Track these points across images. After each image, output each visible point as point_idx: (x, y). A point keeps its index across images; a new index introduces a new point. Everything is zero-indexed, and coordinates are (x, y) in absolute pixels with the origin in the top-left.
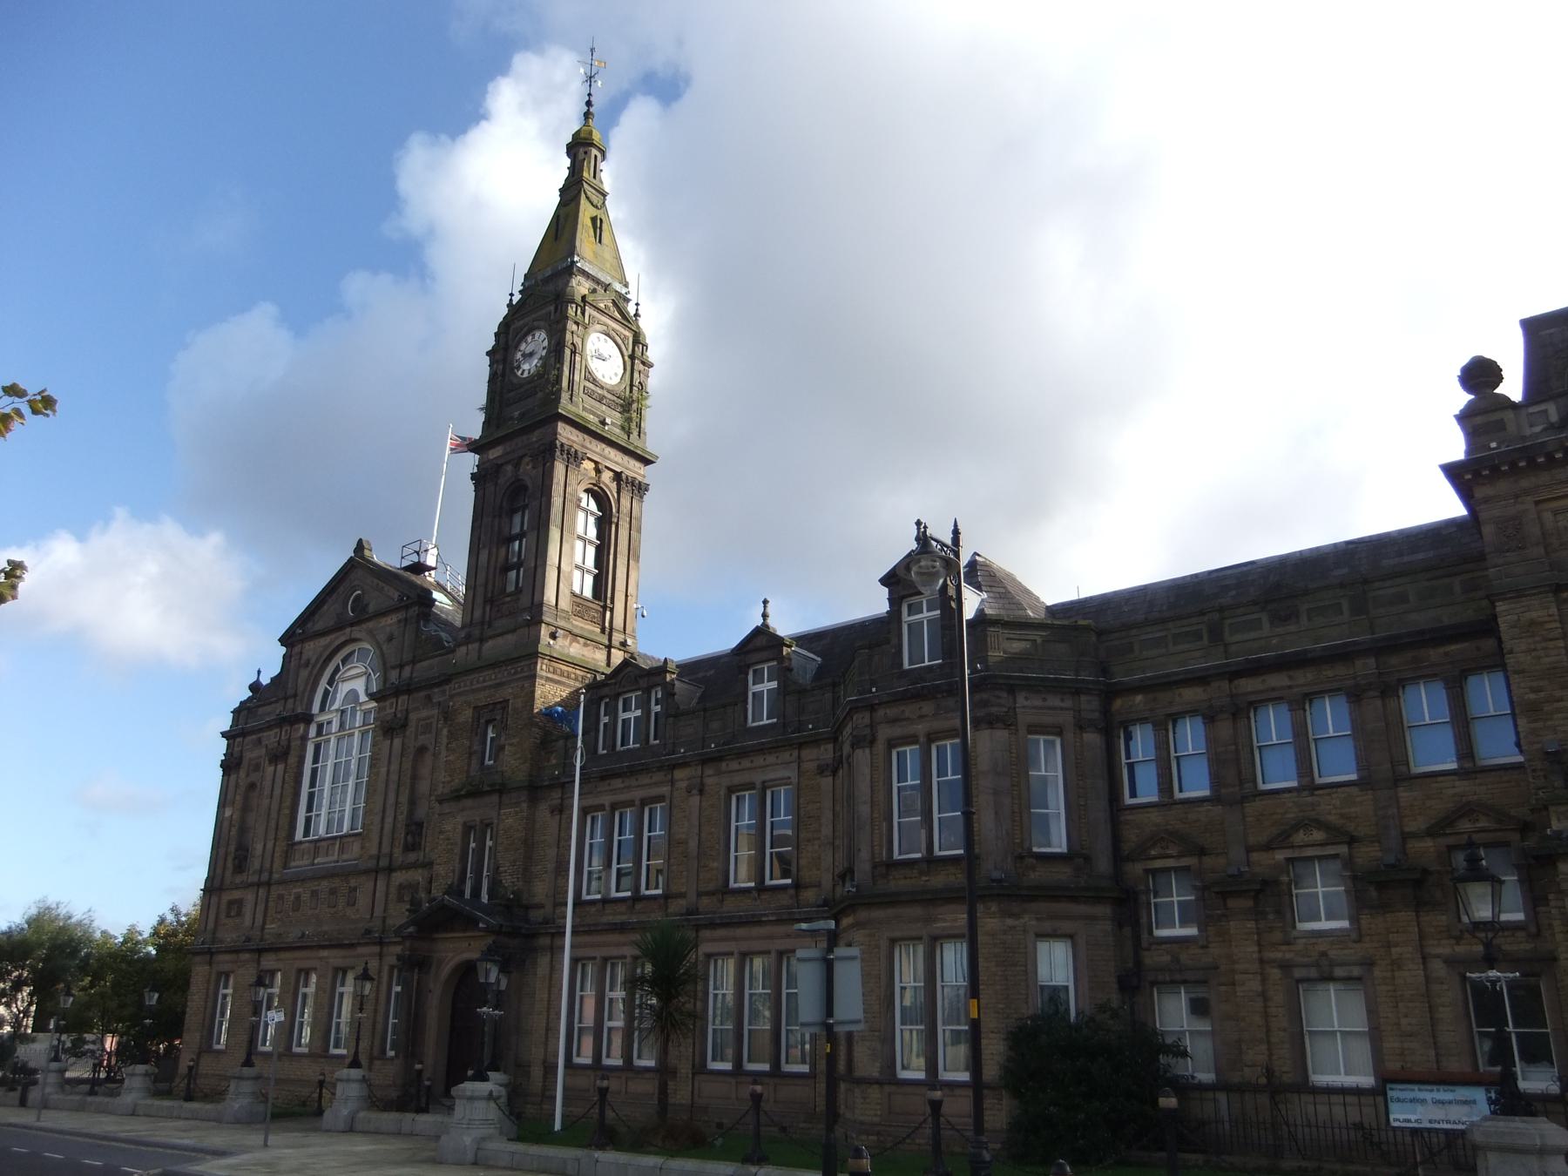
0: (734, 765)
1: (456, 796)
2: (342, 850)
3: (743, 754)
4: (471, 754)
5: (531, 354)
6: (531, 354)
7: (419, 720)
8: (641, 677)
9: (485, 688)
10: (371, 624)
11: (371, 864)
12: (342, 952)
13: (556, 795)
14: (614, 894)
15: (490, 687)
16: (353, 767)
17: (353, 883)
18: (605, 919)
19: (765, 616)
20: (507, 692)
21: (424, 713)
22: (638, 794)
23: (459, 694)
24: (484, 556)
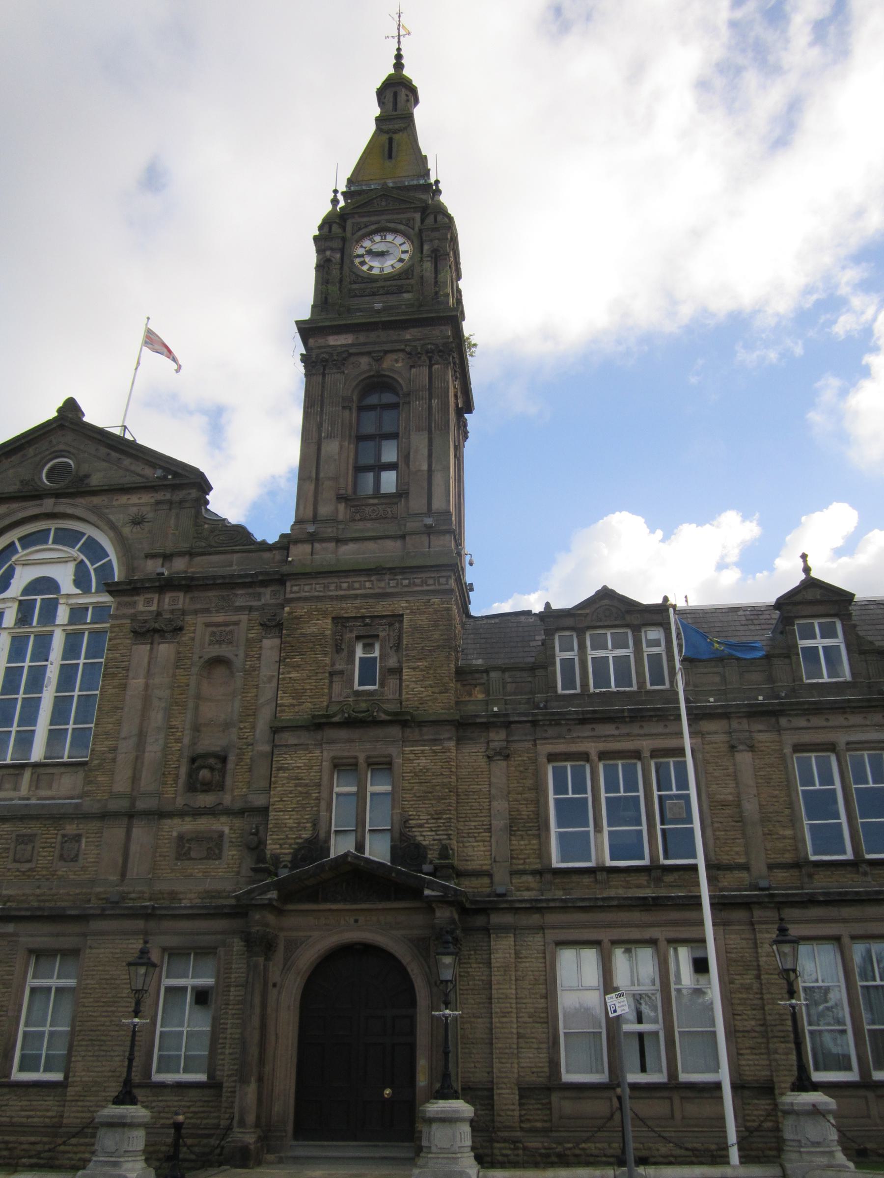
0: (802, 722)
1: (319, 724)
2: (36, 783)
3: (817, 709)
4: (331, 674)
5: (382, 254)
6: (382, 254)
7: (208, 625)
8: (628, 612)
9: (356, 597)
10: (96, 500)
11: (121, 805)
12: (47, 928)
13: (498, 737)
14: (609, 863)
15: (365, 596)
16: (52, 673)
17: (71, 828)
18: (612, 893)
19: (807, 570)
20: (400, 606)
21: (220, 618)
22: (646, 745)
23: (306, 599)
24: (331, 448)
